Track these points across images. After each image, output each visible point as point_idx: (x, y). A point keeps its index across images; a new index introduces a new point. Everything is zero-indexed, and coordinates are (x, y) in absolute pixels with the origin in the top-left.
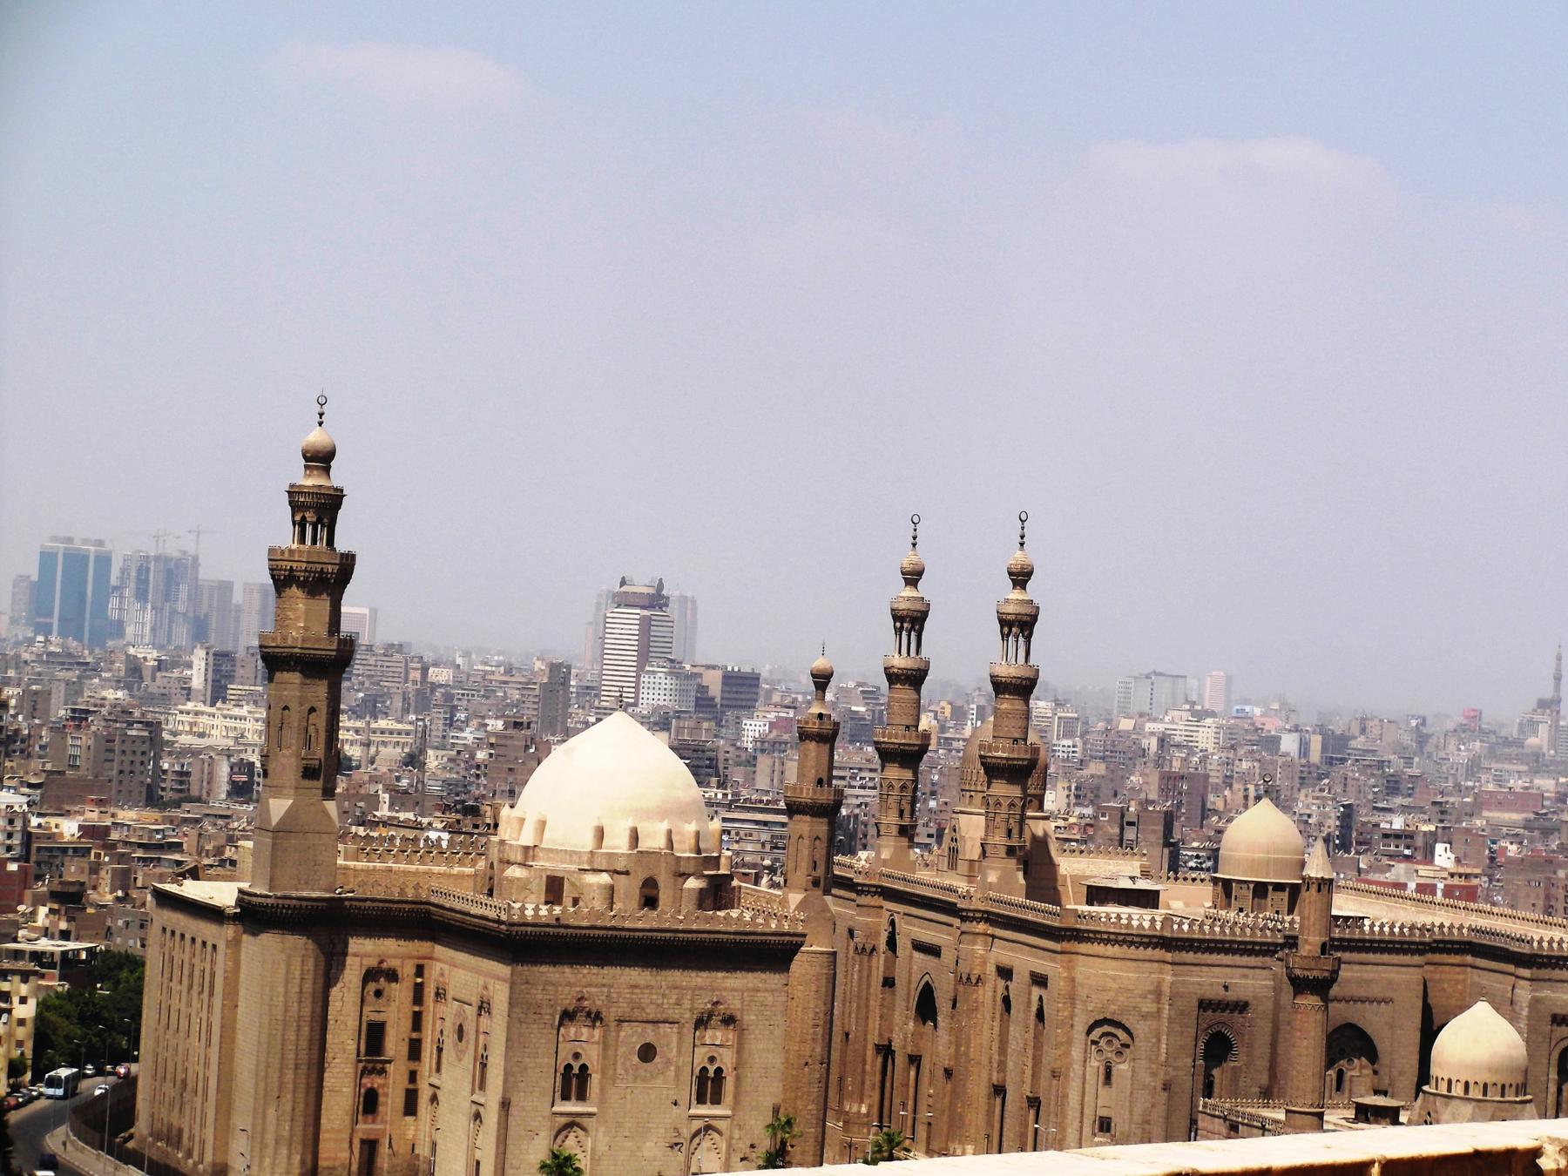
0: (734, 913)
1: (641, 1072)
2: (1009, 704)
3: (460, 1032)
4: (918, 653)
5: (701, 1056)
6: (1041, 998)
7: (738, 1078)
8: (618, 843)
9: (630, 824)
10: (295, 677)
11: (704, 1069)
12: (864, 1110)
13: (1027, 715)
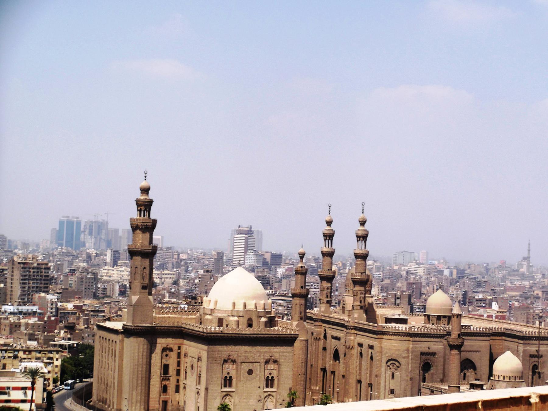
0: (276, 328)
1: (249, 378)
2: (360, 262)
3: (192, 367)
4: (331, 246)
5: (267, 373)
6: (372, 353)
7: (278, 380)
8: (240, 307)
10: (139, 258)
11: (268, 377)
12: (317, 388)
13: (366, 264)
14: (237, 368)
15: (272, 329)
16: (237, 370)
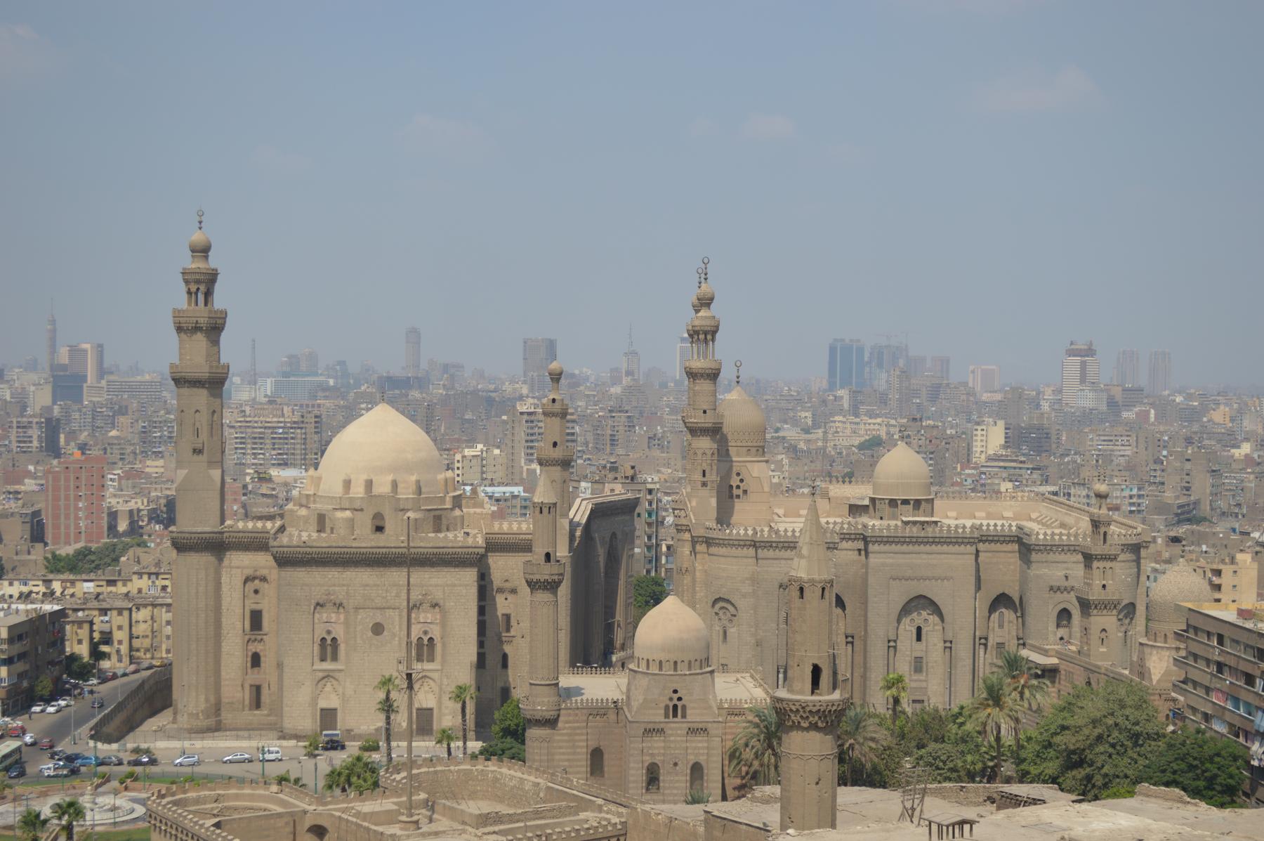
0: (450, 535)
5: (416, 632)
7: (444, 645)
8: (358, 491)
9: (365, 477)
14: (346, 619)
15: (441, 535)
16: (347, 624)
